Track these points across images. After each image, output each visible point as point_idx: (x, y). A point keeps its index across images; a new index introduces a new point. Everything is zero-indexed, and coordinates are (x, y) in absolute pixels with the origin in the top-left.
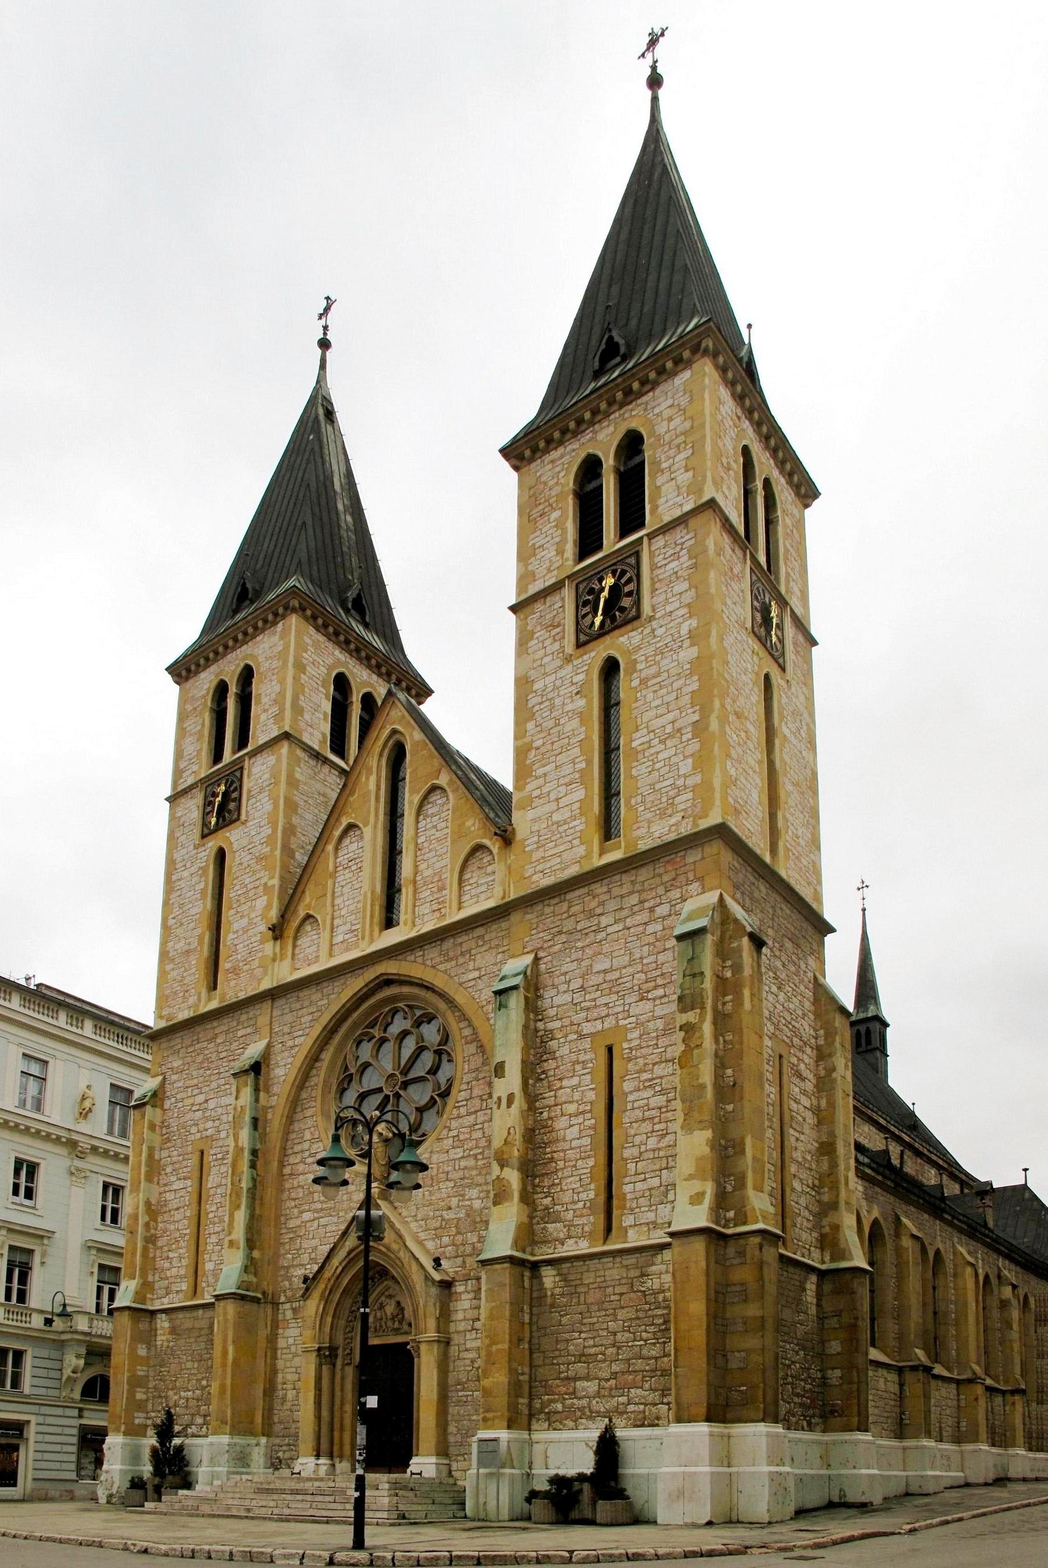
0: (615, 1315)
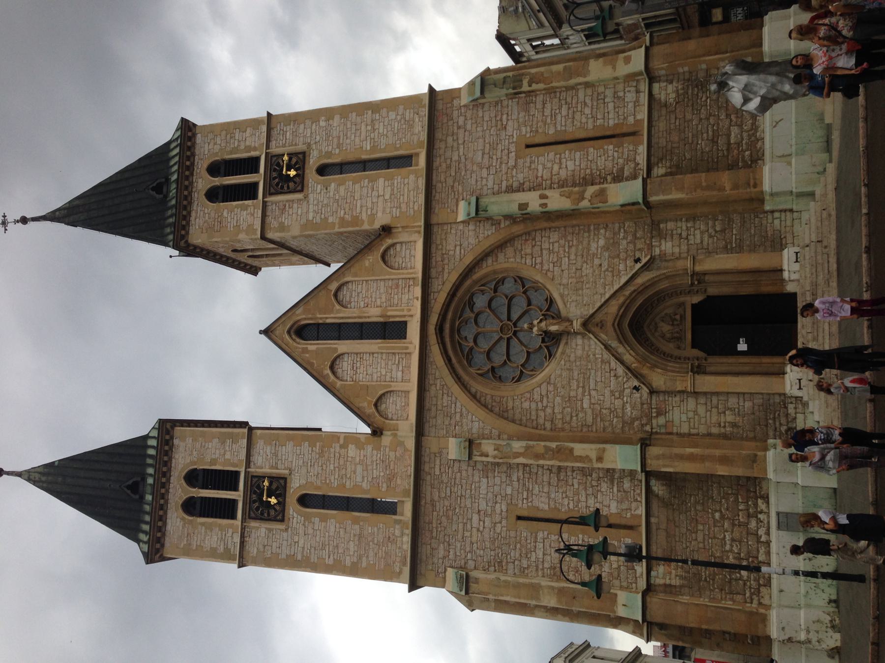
0: (689, 121)
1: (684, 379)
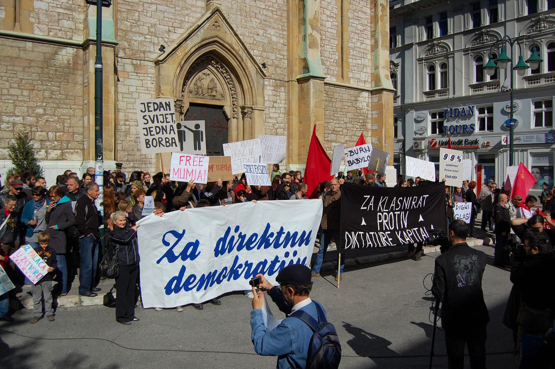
1: (172, 93)
